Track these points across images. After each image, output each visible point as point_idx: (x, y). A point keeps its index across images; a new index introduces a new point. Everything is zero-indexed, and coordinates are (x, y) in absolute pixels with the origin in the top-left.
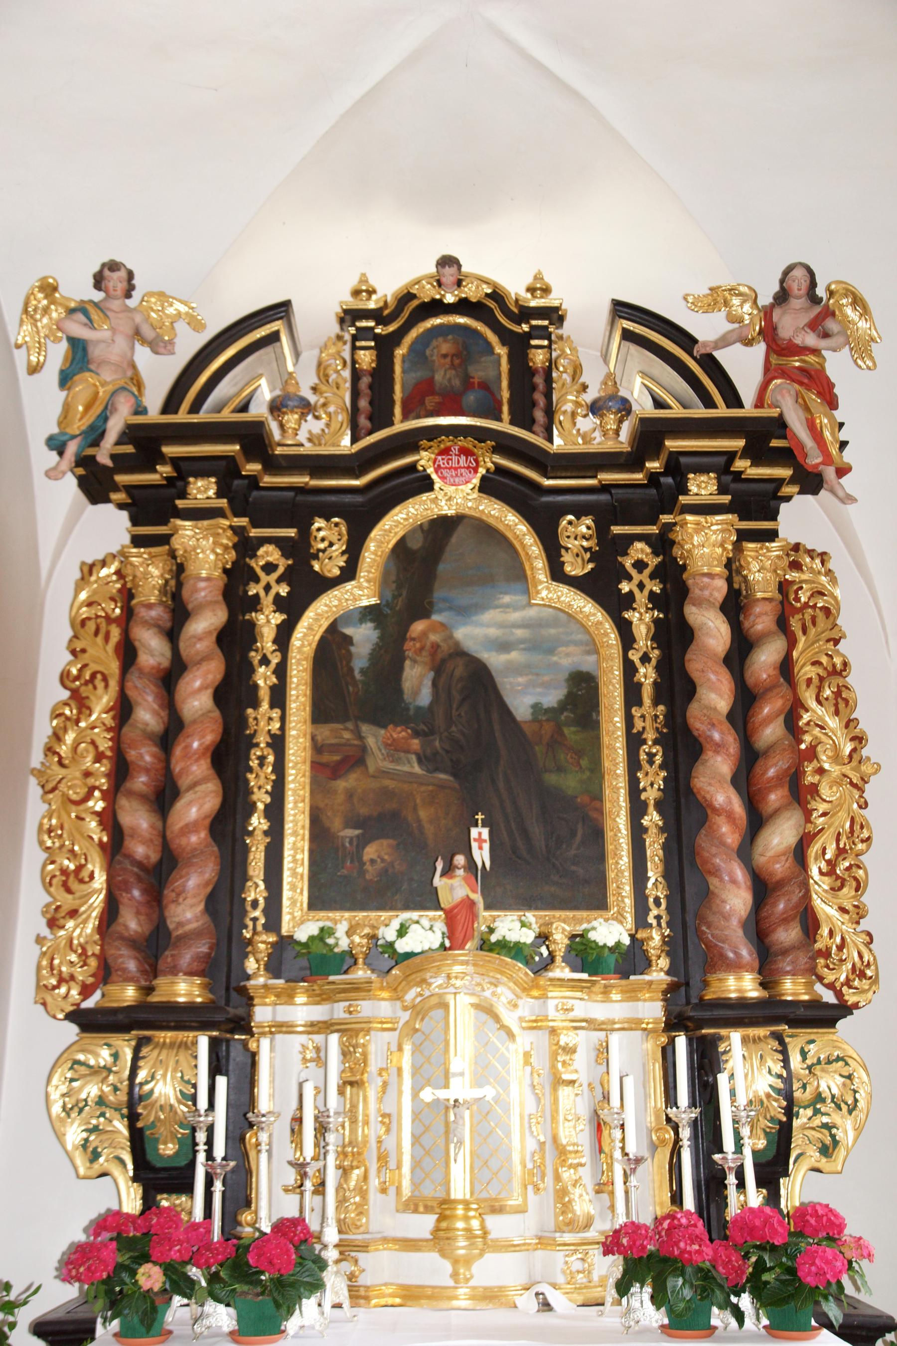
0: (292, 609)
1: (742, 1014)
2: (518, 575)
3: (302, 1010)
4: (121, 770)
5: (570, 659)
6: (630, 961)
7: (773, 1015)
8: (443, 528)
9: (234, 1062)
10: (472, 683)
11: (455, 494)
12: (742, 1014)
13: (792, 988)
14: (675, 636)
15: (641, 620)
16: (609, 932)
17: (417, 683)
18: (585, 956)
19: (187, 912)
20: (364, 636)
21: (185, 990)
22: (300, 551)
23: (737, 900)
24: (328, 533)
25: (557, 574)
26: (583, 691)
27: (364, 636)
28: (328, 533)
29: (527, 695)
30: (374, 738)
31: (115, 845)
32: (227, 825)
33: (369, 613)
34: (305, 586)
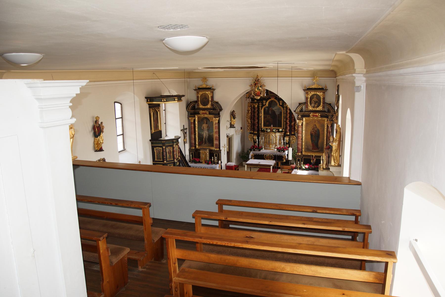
0: (262, 107)
1: (288, 135)
2: (277, 104)
3: (263, 133)
4: (251, 118)
5: (280, 111)
6: (282, 131)
7: (291, 134)
8: (272, 101)
9: (258, 138)
10: (274, 112)
11: (272, 99)
12: (288, 135)
13: (293, 133)
14: (287, 112)
15: (285, 109)
16: (280, 130)
17: (270, 112)
18: (279, 132)
19: (256, 128)
20: (267, 109)
21: (256, 132)
22: (262, 103)
23: (288, 128)
24: (264, 102)
25: (280, 105)
26: (281, 113)
27: (267, 109)
28: (264, 102)
29: (277, 113)
30: (267, 116)
31: (251, 122)
32: (258, 123)
33: (267, 107)
34: (263, 105)
